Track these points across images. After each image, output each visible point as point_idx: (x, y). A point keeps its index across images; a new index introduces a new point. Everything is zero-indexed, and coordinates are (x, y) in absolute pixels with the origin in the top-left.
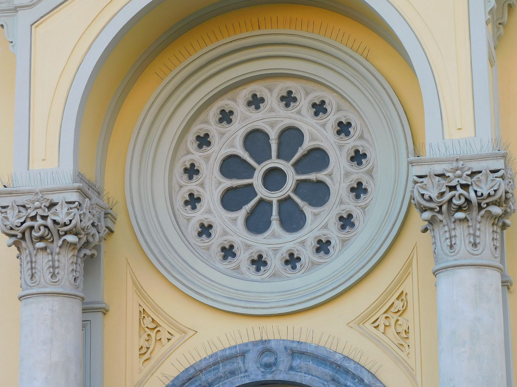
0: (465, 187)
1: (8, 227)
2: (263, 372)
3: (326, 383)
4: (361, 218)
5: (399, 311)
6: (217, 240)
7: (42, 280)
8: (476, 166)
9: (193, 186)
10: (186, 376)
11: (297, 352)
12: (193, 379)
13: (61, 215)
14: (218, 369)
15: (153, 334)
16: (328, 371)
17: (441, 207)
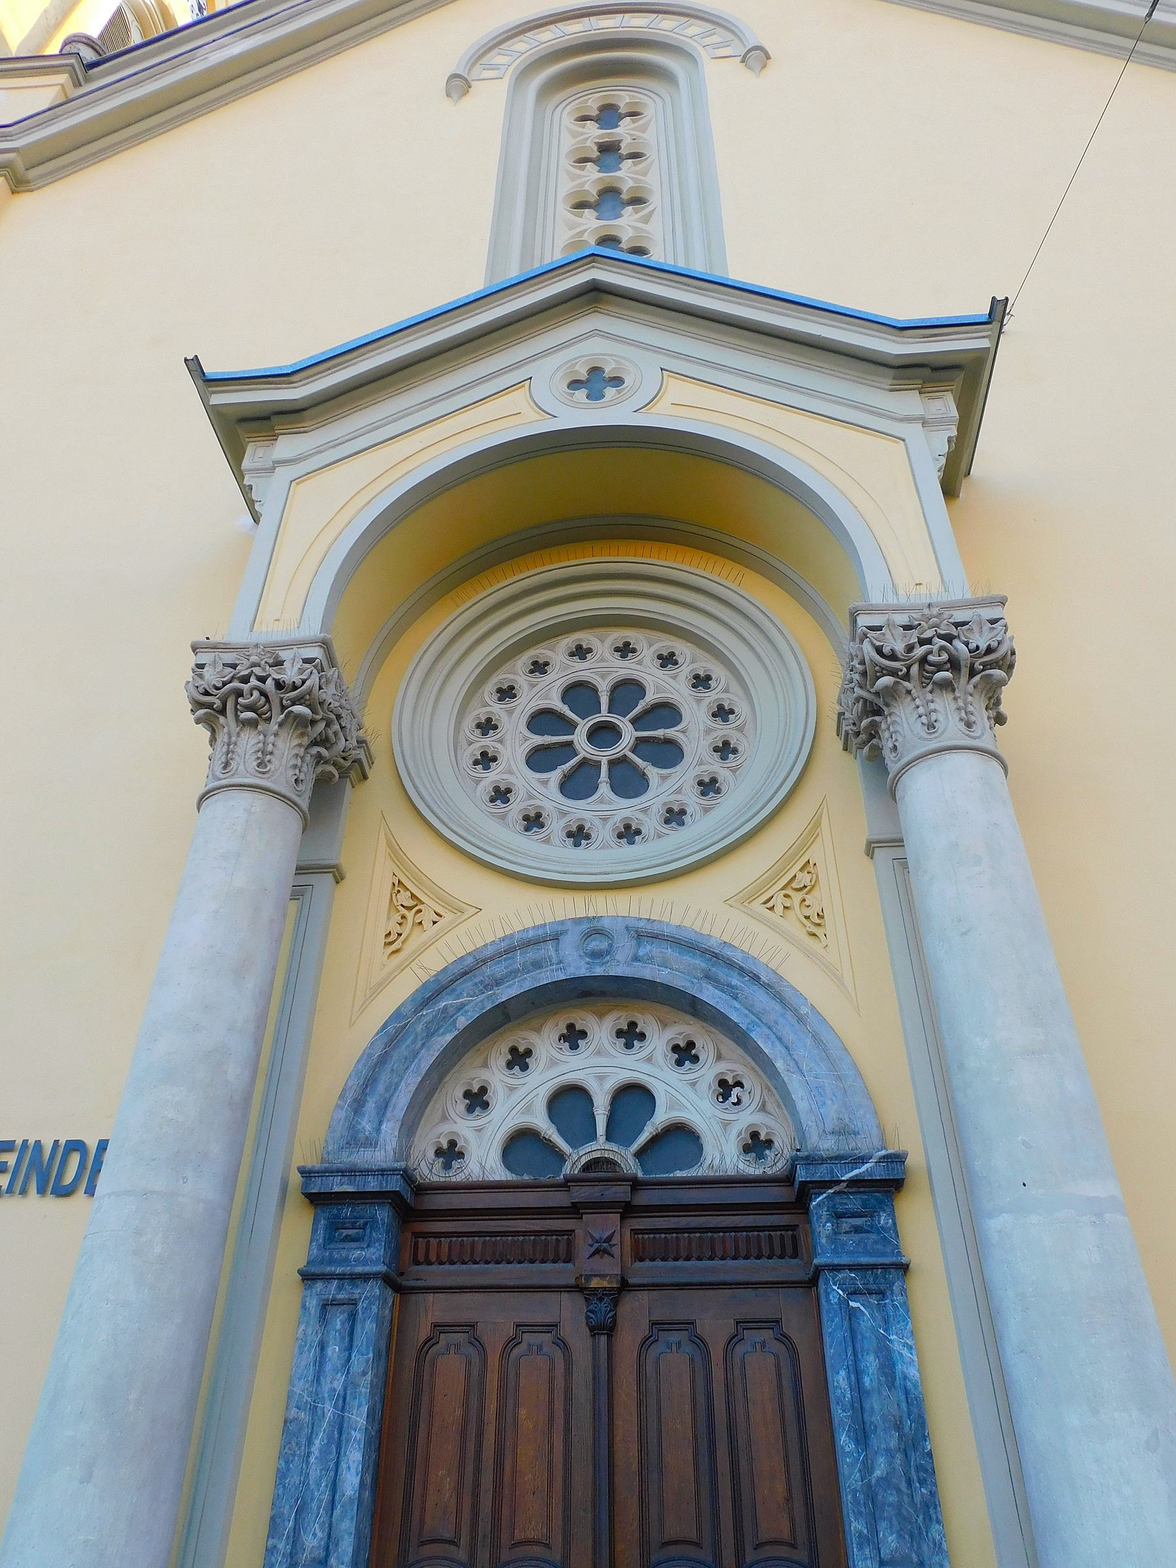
0: (949, 638)
1: (201, 690)
4: (732, 782)
5: (805, 887)
6: (517, 807)
7: (242, 767)
8: (959, 616)
9: (488, 742)
11: (644, 934)
13: (290, 674)
15: (410, 915)
16: (700, 963)
17: (908, 669)
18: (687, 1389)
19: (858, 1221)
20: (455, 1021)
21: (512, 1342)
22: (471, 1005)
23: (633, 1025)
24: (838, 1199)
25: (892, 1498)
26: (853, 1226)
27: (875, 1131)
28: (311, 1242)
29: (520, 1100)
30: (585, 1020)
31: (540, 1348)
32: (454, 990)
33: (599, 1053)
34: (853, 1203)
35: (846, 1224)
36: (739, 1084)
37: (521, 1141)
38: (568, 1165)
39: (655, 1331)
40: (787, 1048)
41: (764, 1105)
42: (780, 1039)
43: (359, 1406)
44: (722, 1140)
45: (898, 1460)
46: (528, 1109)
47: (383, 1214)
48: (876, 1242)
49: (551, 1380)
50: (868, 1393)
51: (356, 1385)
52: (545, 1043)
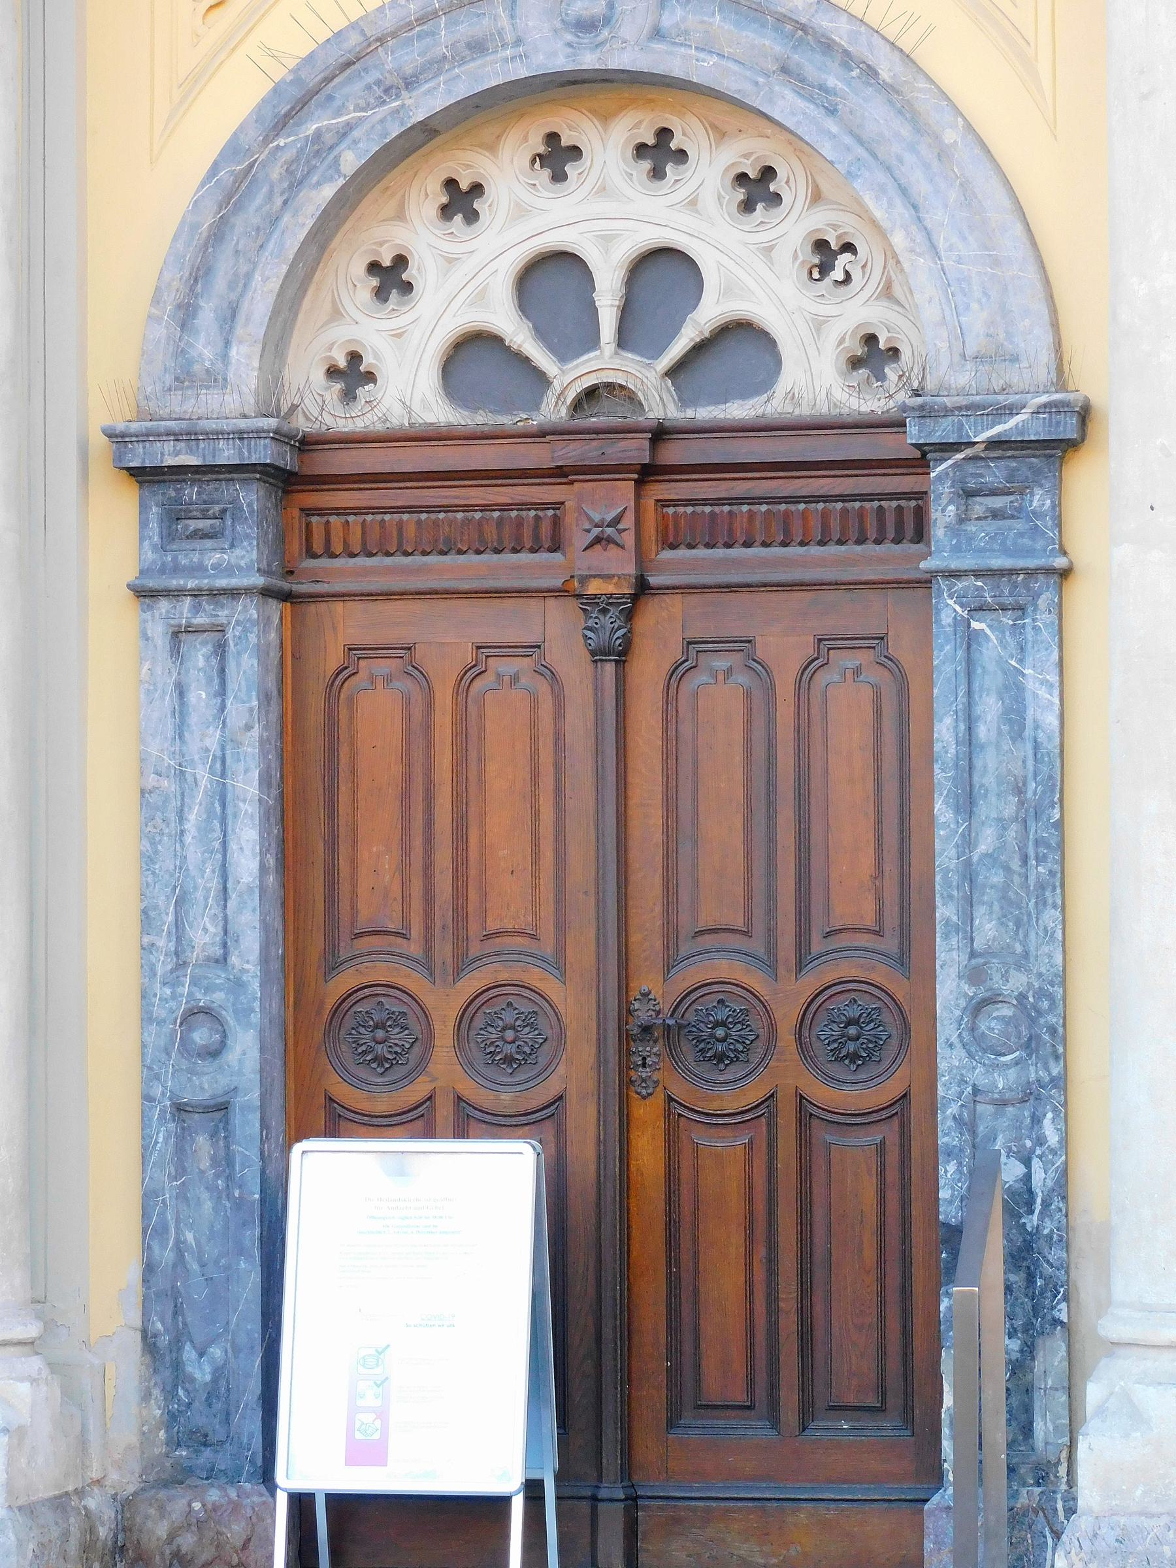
2: (570, 45)
3: (761, 80)
10: (335, 57)
12: (357, 66)
14: (432, 34)
18: (738, 736)
19: (997, 502)
20: (336, 160)
21: (472, 672)
22: (364, 126)
23: (664, 134)
24: (970, 468)
25: (997, 878)
26: (988, 509)
27: (1045, 357)
28: (142, 539)
29: (467, 280)
30: (576, 128)
31: (515, 679)
32: (330, 98)
33: (602, 190)
34: (994, 473)
35: (980, 506)
36: (849, 247)
37: (471, 353)
38: (551, 397)
39: (692, 653)
40: (915, 207)
41: (888, 286)
42: (904, 191)
43: (246, 771)
44: (812, 352)
45: (1013, 832)
46: (481, 297)
47: (250, 497)
48: (1021, 535)
49: (534, 724)
50: (982, 747)
51: (238, 744)
52: (505, 170)
